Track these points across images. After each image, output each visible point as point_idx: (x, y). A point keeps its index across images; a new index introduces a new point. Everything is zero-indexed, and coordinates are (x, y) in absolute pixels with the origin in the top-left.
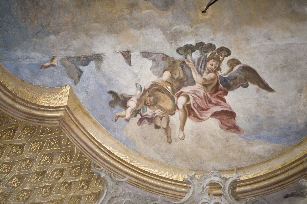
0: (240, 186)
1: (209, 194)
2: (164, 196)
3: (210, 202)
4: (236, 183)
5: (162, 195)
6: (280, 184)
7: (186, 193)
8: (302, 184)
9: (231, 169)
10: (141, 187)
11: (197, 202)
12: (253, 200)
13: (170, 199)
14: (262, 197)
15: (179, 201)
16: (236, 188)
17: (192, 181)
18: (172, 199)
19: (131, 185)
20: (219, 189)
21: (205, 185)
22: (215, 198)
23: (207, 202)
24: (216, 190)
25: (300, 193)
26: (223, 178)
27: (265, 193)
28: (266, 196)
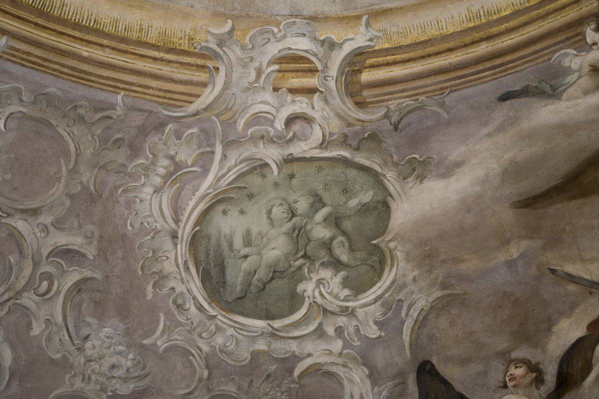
0: (373, 66)
1: (276, 90)
2: (133, 94)
3: (277, 111)
4: (364, 57)
5: (127, 93)
6: (497, 62)
7: (204, 85)
8: (560, 62)
9: (351, 13)
10: (54, 70)
11: (236, 112)
12: (407, 105)
13: (154, 104)
14: (436, 97)
15: (182, 109)
16: (360, 71)
17: (225, 49)
18: (161, 104)
19: (18, 66)
20: (310, 74)
21: (265, 64)
22: (293, 101)
23: (267, 113)
24: (297, 77)
25: (547, 88)
26: (323, 42)
27: (447, 88)
28: (448, 94)
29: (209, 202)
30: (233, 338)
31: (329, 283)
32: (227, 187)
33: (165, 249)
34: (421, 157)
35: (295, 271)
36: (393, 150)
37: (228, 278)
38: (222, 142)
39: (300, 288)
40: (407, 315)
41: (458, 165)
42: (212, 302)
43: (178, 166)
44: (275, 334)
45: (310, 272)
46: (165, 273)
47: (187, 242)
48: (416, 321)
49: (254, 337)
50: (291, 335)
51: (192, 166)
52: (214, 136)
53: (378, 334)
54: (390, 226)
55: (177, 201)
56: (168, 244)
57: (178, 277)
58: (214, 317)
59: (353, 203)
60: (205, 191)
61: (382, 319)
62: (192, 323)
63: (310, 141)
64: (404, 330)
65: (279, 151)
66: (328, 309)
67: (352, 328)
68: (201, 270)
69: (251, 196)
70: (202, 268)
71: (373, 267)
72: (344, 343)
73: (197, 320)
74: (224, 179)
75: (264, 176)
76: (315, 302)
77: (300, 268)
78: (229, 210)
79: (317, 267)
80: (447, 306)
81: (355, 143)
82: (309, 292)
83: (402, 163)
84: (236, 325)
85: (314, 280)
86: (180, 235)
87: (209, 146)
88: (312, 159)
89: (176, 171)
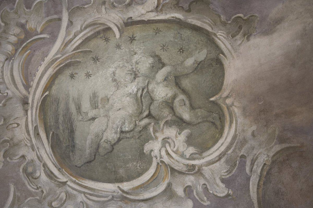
29: (57, 67)
30: (83, 205)
31: (174, 142)
32: (74, 52)
33: (16, 116)
34: (245, 16)
35: (141, 131)
36: (220, 10)
37: (77, 141)
38: (68, 9)
39: (147, 148)
40: (251, 171)
41: (279, 21)
42: (62, 168)
43: (28, 34)
44: (126, 198)
45: (155, 131)
46: (15, 141)
47: (37, 107)
48: (260, 177)
49: (104, 202)
50: (141, 198)
51: (41, 33)
52: (61, 4)
53: (226, 192)
54: (225, 83)
55: (27, 68)
56: (19, 112)
57: (29, 145)
58: (64, 183)
59: (190, 62)
60: (54, 56)
61: (228, 176)
62: (42, 192)
63: (146, 4)
64: (251, 186)
65: (120, 15)
66: (176, 168)
67: (201, 187)
68: (51, 135)
69: (96, 59)
70: (52, 133)
71: (213, 123)
72: (194, 204)
73: (47, 188)
74: (71, 44)
75: (107, 40)
76: (162, 162)
77: (145, 127)
78: (77, 74)
79: (162, 126)
80: (287, 160)
81: (186, 6)
82: (156, 153)
83: (229, 22)
84: (86, 191)
85: (160, 139)
86: (30, 101)
87: (56, 13)
88: (150, 22)
89: (26, 38)
